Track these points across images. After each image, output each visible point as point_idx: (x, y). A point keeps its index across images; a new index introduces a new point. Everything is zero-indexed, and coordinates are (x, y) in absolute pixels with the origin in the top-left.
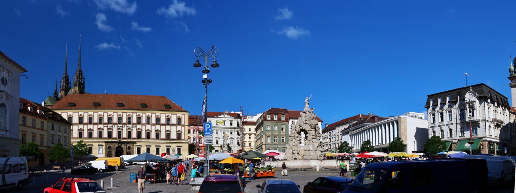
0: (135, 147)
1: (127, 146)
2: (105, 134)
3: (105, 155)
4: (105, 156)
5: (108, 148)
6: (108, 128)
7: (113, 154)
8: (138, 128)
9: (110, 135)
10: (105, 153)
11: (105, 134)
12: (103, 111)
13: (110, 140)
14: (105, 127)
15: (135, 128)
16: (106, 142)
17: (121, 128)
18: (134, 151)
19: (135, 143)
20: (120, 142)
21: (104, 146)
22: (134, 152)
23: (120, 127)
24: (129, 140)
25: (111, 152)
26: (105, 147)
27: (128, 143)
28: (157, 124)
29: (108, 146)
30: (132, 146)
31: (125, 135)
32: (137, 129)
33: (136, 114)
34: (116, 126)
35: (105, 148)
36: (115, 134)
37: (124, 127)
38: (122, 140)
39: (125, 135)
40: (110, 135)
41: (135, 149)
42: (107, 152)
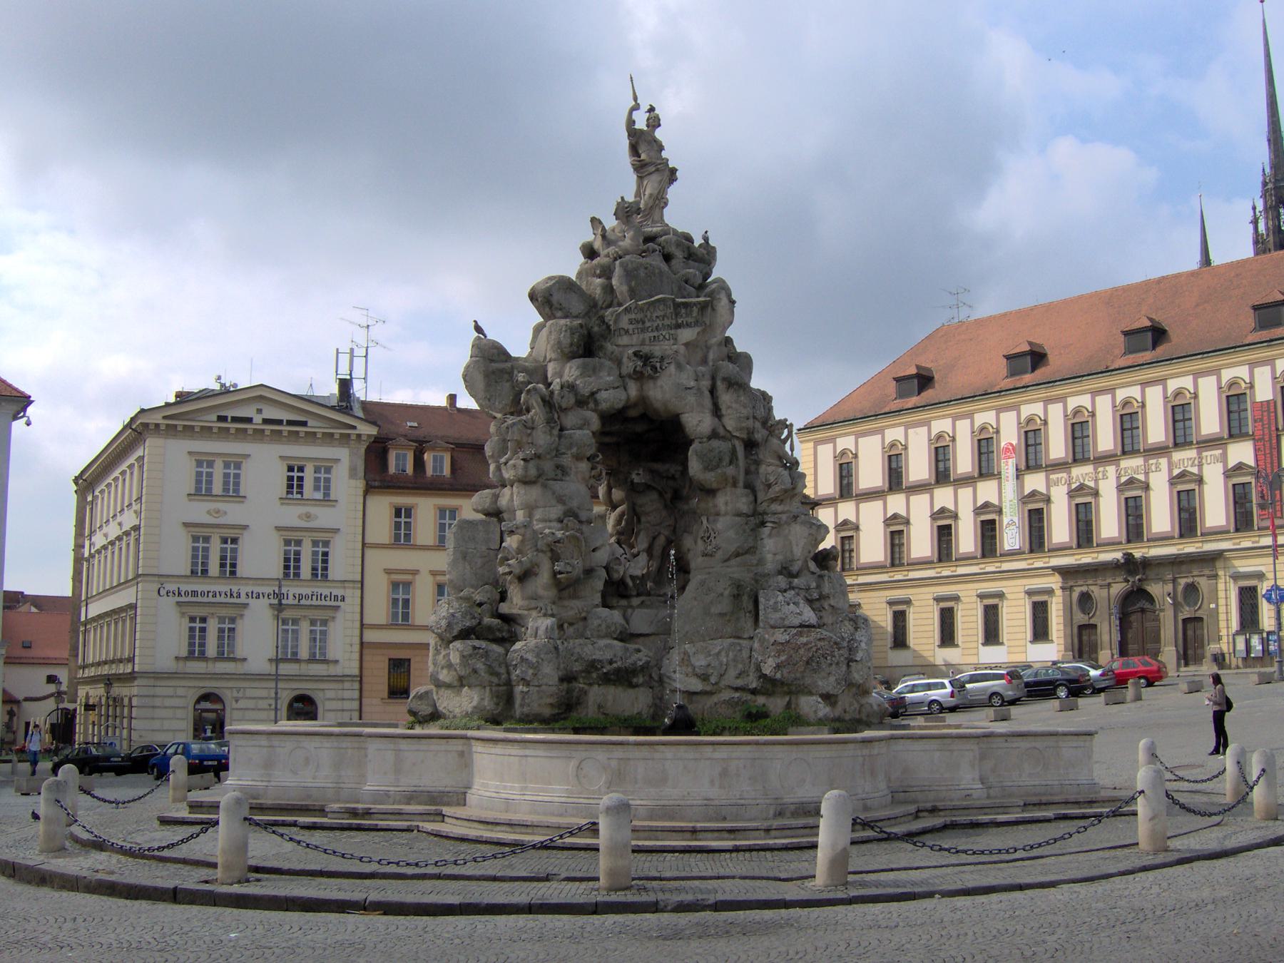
0: (1221, 586)
1: (1174, 580)
2: (1060, 528)
3: (1062, 648)
4: (1066, 650)
5: (1075, 607)
6: (1074, 486)
7: (1106, 638)
8: (1232, 463)
9: (1085, 530)
10: (1062, 634)
11: (1060, 528)
12: (1043, 393)
13: (1086, 558)
14: (1057, 483)
15: (1219, 468)
16: (1065, 572)
17: (1141, 477)
18: (1222, 609)
19: (1216, 556)
20: (1130, 565)
21: (1059, 592)
22: (1222, 617)
23: (1136, 471)
24: (1190, 548)
25: (1096, 626)
26: (1061, 600)
27: (1177, 562)
28: (1231, 436)
29: (1075, 595)
30: (1203, 583)
31: (1161, 517)
32: (1228, 474)
33: (1213, 379)
34: (1111, 470)
35: (1061, 606)
36: (1109, 523)
37: (1158, 469)
38: (1138, 554)
39: (1161, 517)
40: (1085, 530)
41: (1222, 602)
42: (1075, 630)
